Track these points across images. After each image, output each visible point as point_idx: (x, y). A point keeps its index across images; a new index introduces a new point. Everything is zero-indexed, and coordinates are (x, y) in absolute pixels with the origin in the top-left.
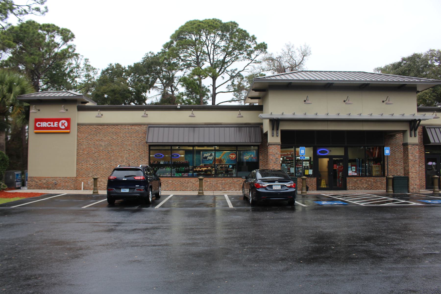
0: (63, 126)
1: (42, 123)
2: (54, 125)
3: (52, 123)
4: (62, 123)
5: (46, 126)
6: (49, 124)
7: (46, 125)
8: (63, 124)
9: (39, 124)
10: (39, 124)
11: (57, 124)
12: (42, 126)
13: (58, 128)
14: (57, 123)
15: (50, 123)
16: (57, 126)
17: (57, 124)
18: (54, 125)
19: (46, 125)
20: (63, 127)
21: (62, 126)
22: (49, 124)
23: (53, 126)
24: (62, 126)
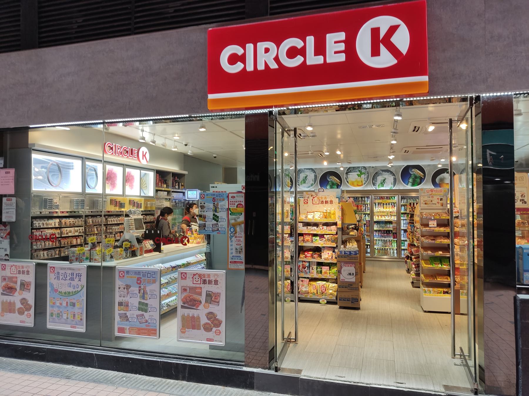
0: (383, 49)
1: (250, 47)
3: (310, 40)
4: (375, 32)
5: (274, 66)
6: (292, 53)
9: (233, 59)
10: (233, 59)
12: (250, 68)
14: (342, 36)
15: (296, 42)
16: (342, 58)
18: (320, 49)
21: (375, 52)
22: (292, 53)
23: (320, 60)
24: (375, 52)
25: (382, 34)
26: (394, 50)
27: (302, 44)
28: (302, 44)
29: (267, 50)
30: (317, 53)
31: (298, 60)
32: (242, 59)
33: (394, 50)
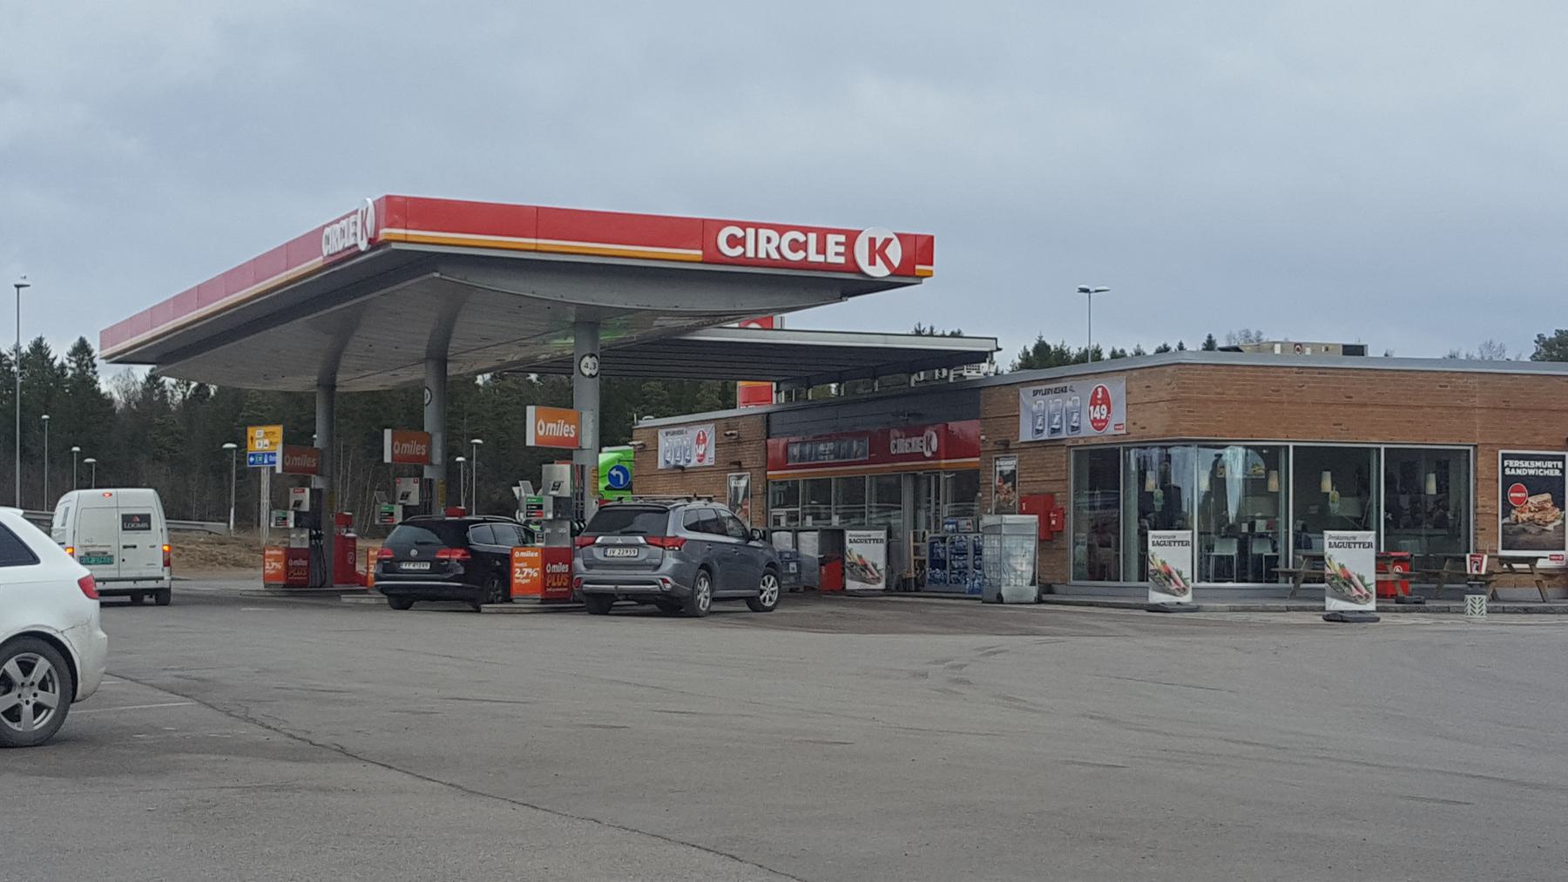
4: (872, 241)
5: (775, 255)
6: (795, 246)
7: (778, 249)
10: (733, 241)
11: (842, 249)
12: (750, 254)
15: (801, 238)
16: (841, 260)
17: (842, 249)
18: (822, 249)
19: (778, 249)
21: (872, 262)
23: (821, 258)
24: (872, 262)
25: (878, 245)
27: (804, 239)
28: (804, 239)
29: (769, 240)
31: (800, 255)
32: (742, 242)
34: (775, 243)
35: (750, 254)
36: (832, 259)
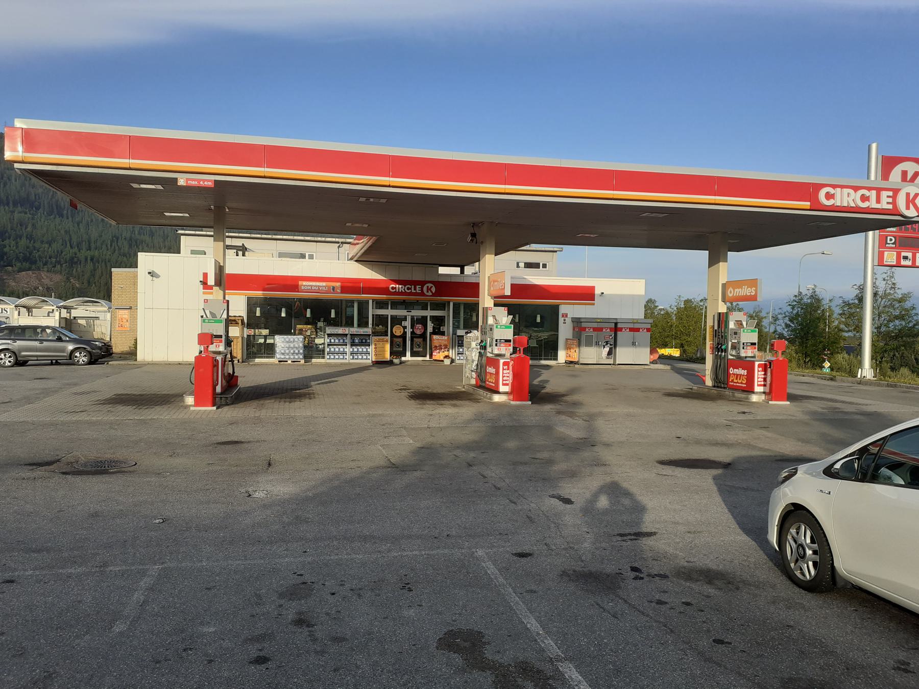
2: (415, 289)
3: (413, 286)
4: (428, 287)
5: (403, 291)
6: (408, 289)
7: (404, 289)
8: (429, 289)
13: (422, 294)
14: (420, 286)
16: (420, 291)
18: (415, 289)
19: (404, 289)
20: (430, 294)
21: (428, 292)
22: (408, 289)
23: (415, 291)
24: (428, 292)
26: (432, 292)
30: (414, 290)
33: (432, 292)
34: (403, 288)
35: (397, 291)
36: (418, 291)
